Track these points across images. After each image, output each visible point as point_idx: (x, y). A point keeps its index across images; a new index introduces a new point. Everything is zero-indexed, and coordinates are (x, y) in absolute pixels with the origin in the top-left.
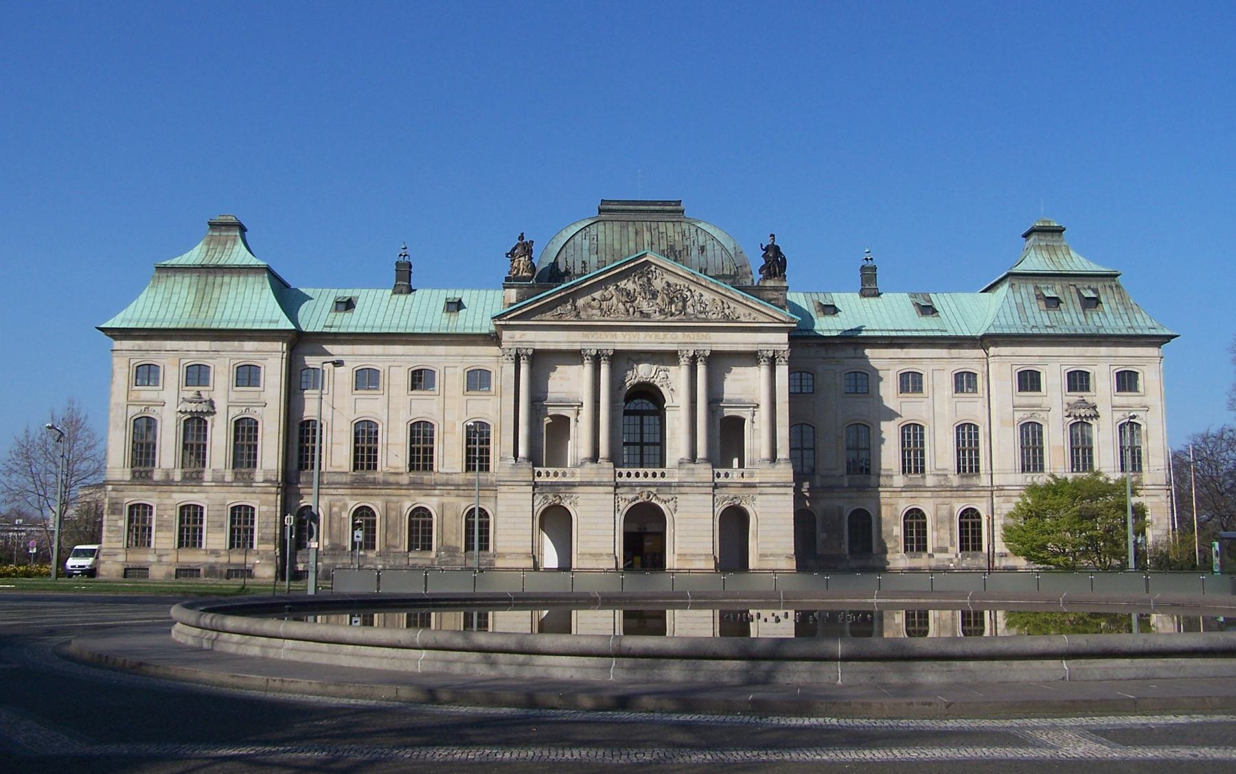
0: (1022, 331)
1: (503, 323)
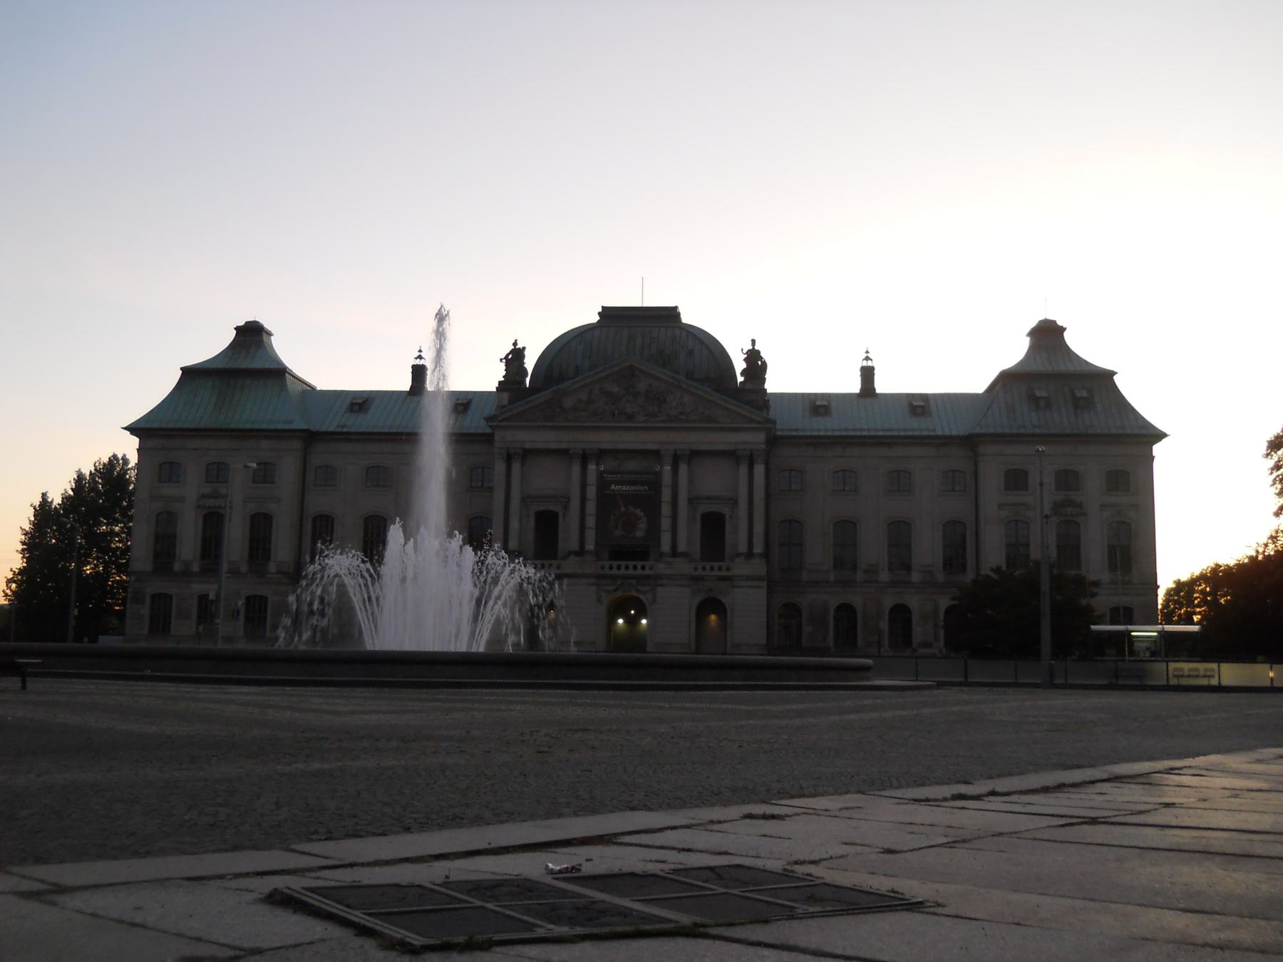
0: (1007, 431)
1: (496, 424)
